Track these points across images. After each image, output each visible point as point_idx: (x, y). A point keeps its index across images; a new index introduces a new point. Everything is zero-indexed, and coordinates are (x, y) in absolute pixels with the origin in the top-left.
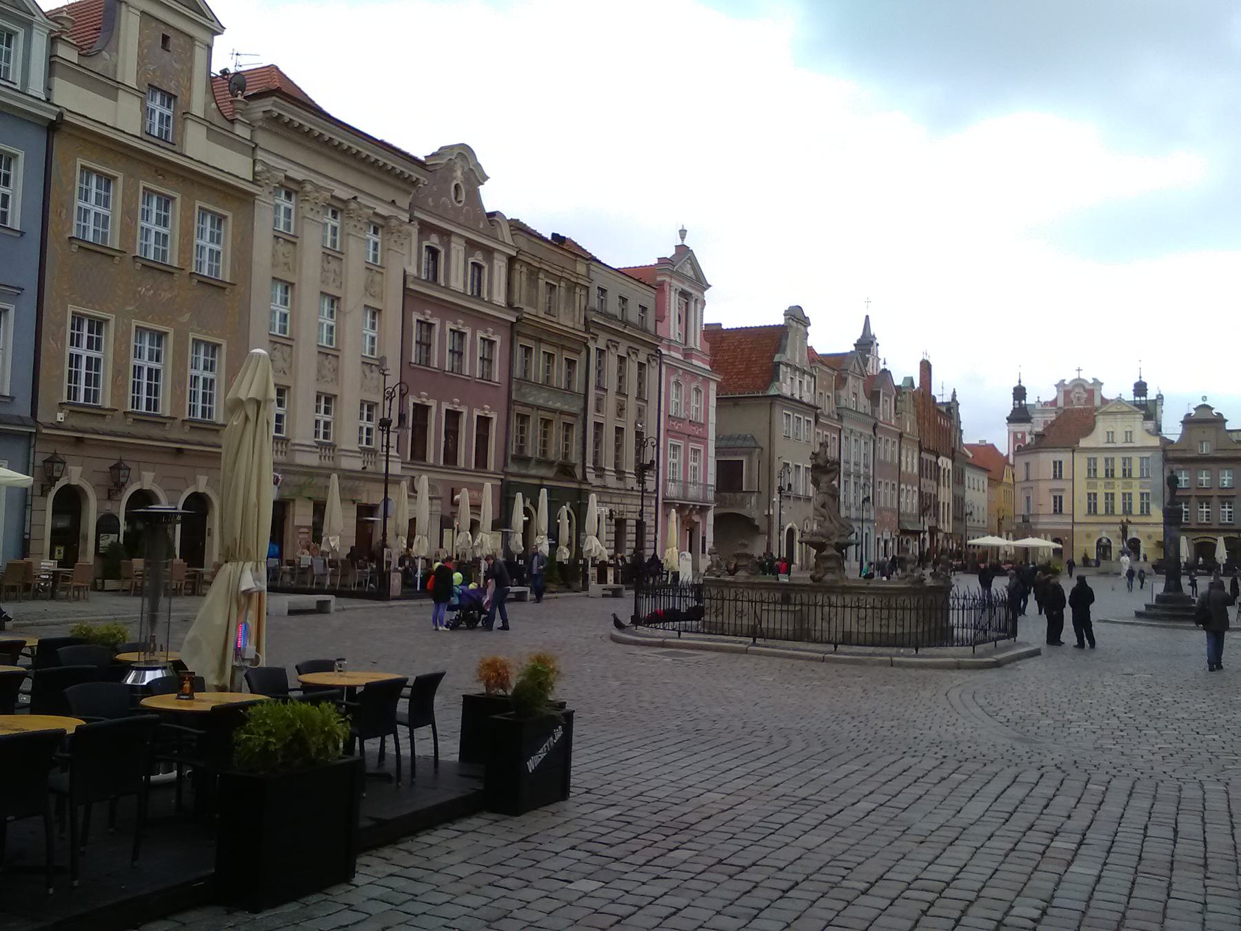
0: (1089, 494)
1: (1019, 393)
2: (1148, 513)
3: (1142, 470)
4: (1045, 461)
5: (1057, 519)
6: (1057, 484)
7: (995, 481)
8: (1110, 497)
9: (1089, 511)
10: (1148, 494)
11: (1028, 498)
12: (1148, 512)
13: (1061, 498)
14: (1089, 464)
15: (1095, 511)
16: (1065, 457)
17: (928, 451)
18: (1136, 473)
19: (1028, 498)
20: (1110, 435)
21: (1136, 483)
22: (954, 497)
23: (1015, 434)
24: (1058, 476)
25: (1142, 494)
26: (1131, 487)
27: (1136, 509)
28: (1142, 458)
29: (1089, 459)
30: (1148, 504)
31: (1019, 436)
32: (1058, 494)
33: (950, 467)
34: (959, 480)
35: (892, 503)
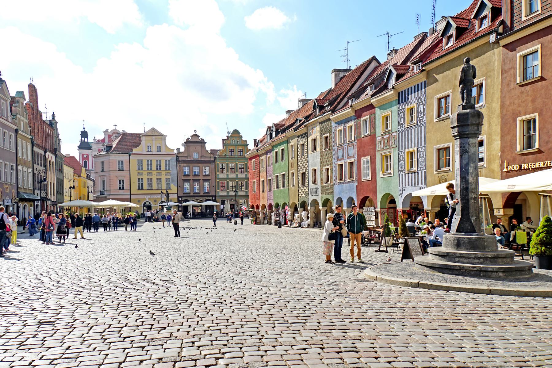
0: (139, 179)
1: (84, 134)
3: (166, 166)
5: (121, 192)
6: (121, 173)
7: (77, 173)
8: (150, 181)
10: (169, 179)
11: (103, 181)
13: (123, 181)
17: (38, 146)
19: (103, 181)
20: (149, 148)
22: (57, 179)
23: (83, 155)
25: (167, 179)
30: (170, 184)
31: (85, 156)
32: (121, 179)
33: (54, 160)
34: (60, 170)
35: (11, 179)
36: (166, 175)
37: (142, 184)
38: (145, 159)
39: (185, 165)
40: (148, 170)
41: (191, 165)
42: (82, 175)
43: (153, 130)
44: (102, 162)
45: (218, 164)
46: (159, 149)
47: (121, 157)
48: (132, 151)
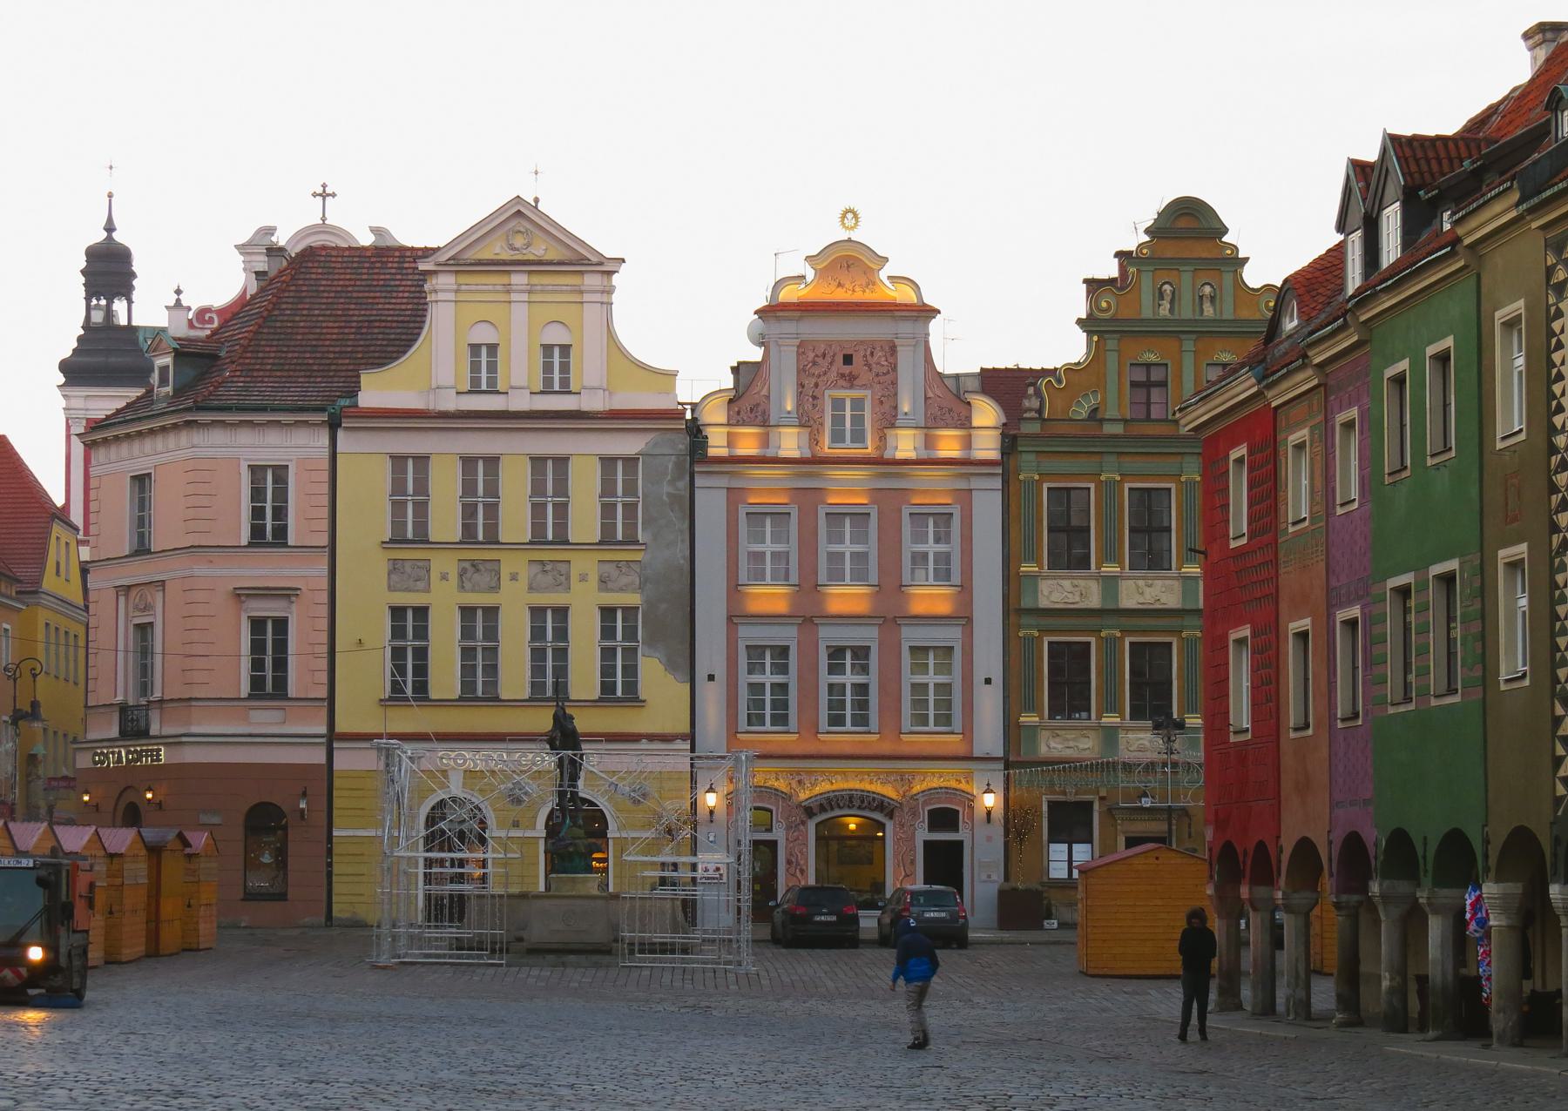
1: (109, 270)
2: (632, 697)
3: (608, 510)
4: (214, 462)
5: (265, 719)
6: (268, 569)
8: (480, 623)
9: (397, 687)
10: (630, 612)
12: (631, 687)
13: (281, 625)
14: (398, 486)
15: (421, 688)
16: (297, 447)
18: (585, 522)
19: (144, 630)
20: (482, 358)
21: (585, 565)
24: (269, 533)
25: (608, 613)
26: (563, 583)
27: (584, 679)
28: (608, 462)
29: (398, 460)
30: (630, 653)
32: (269, 609)
36: (604, 583)
37: (421, 654)
38: (445, 454)
42: (49, 582)
43: (520, 215)
44: (141, 481)
46: (557, 361)
47: (273, 438)
48: (353, 391)
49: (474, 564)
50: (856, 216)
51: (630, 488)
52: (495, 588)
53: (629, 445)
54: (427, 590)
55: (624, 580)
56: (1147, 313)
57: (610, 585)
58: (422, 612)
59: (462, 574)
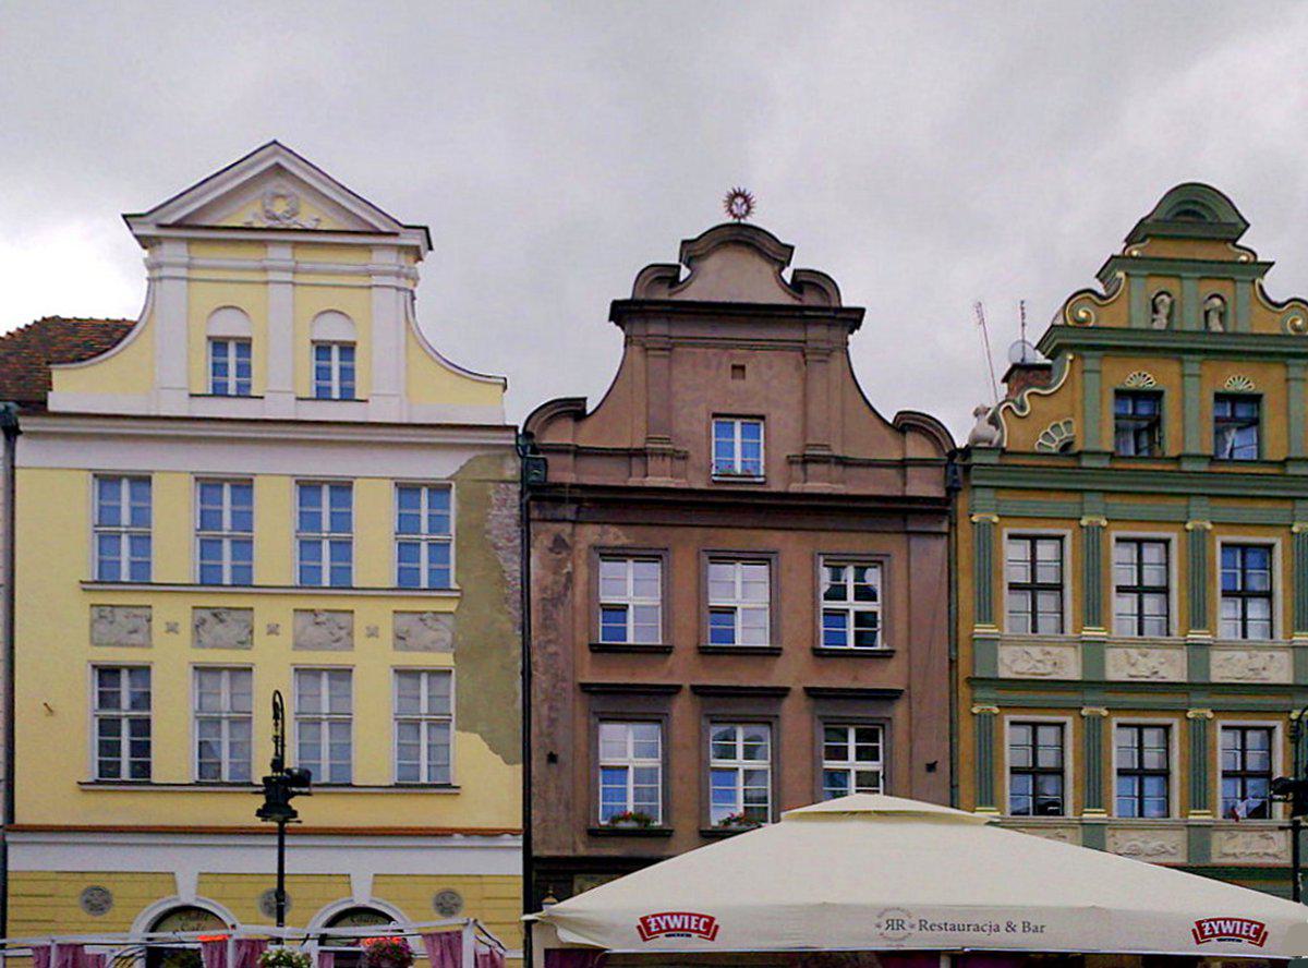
3: (407, 550)
9: (108, 771)
15: (142, 770)
18: (374, 560)
21: (374, 616)
26: (344, 639)
28: (407, 490)
37: (142, 727)
39: (615, 536)
40: (209, 579)
41: (687, 541)
45: (985, 533)
46: (334, 360)
49: (216, 614)
50: (747, 199)
51: (438, 523)
52: (245, 644)
53: (440, 467)
54: (147, 644)
55: (430, 635)
56: (1140, 322)
57: (410, 641)
58: (141, 672)
59: (198, 626)
